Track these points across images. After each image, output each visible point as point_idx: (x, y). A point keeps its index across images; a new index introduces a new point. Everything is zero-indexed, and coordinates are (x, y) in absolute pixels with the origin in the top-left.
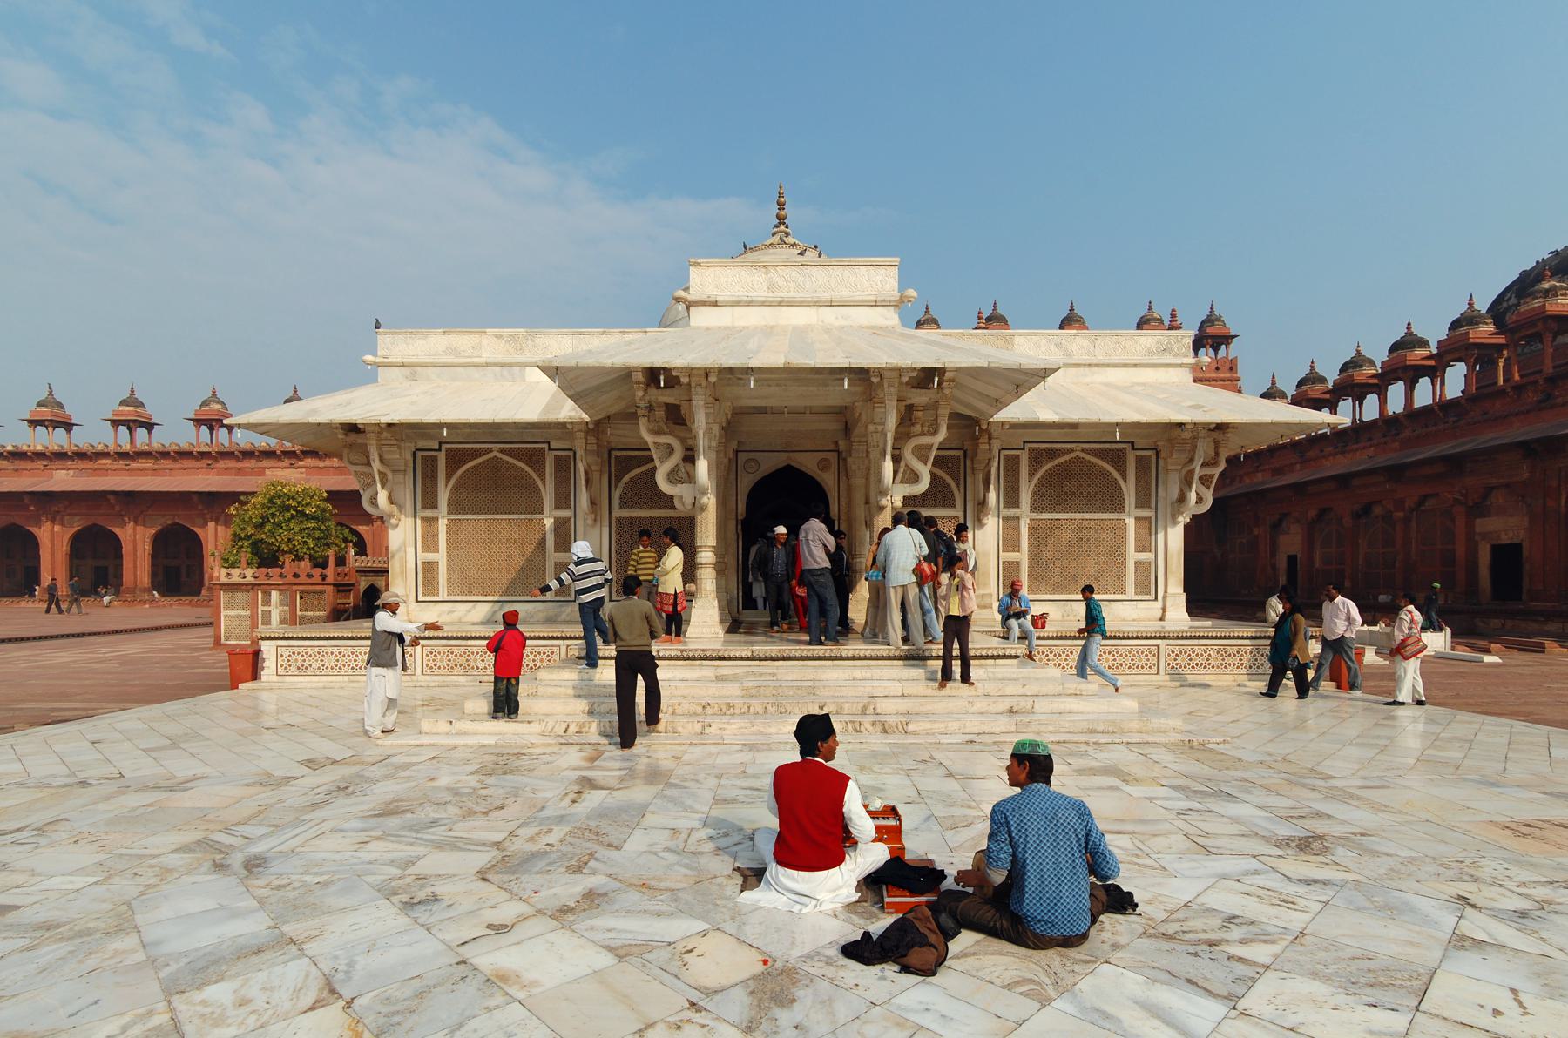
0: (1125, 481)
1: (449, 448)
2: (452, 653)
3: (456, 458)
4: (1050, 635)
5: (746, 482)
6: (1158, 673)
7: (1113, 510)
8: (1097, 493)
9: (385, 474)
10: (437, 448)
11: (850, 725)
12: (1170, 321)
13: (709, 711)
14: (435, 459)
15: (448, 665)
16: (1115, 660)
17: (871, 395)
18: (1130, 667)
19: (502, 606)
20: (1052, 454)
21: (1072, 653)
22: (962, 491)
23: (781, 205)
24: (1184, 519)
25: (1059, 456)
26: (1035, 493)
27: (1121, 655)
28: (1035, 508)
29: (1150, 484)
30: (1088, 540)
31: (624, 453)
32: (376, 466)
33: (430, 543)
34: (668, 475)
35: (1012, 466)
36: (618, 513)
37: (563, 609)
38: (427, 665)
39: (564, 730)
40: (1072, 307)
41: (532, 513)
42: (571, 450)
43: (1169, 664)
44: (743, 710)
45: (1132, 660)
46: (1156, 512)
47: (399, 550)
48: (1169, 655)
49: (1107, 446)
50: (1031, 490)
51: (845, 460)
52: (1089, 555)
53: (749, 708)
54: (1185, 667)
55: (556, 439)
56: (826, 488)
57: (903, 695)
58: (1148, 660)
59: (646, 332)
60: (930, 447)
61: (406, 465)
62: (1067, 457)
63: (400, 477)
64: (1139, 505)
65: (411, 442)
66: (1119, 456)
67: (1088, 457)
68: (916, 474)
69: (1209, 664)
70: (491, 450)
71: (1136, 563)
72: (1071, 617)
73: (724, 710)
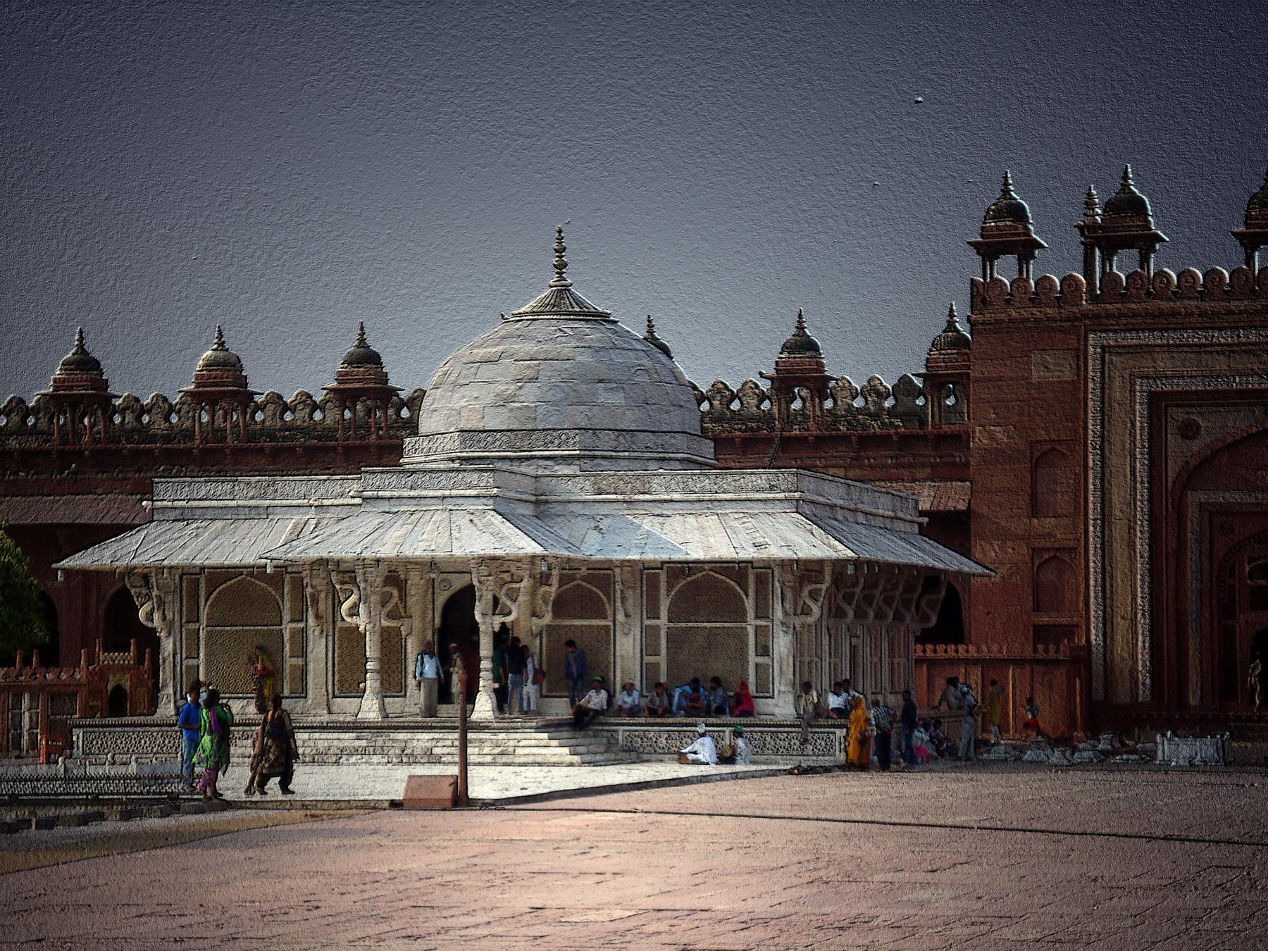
0: (747, 595)
5: (441, 599)
14: (198, 582)
22: (612, 604)
23: (560, 251)
50: (668, 604)
62: (699, 575)
64: (757, 617)
70: (241, 574)
71: (757, 665)
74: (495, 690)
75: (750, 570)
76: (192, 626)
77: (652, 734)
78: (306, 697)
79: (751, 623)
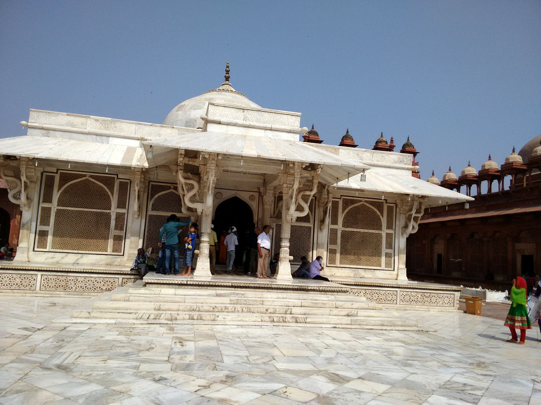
0: (383, 217)
1: (62, 173)
2: (58, 279)
3: (65, 178)
4: (352, 283)
6: (396, 304)
7: (377, 229)
8: (370, 221)
9: (27, 183)
10: (56, 172)
11: (281, 318)
12: (390, 143)
13: (216, 310)
14: (53, 178)
15: (55, 286)
16: (378, 297)
17: (286, 171)
18: (385, 300)
19: (82, 256)
20: (353, 202)
21: (360, 292)
24: (406, 236)
25: (356, 203)
26: (344, 219)
27: (381, 295)
28: (344, 226)
29: (393, 219)
30: (366, 241)
31: (156, 184)
32: (23, 179)
33: (45, 221)
34: (191, 197)
35: (335, 205)
36: (150, 212)
37: (116, 260)
38: (43, 285)
39: (147, 317)
40: (348, 131)
41: (105, 209)
42: (129, 180)
43: (401, 300)
44: (232, 310)
45: (386, 297)
46: (395, 231)
47: (26, 223)
48: (401, 296)
49: (376, 200)
51: (262, 197)
52: (366, 249)
53: (235, 309)
54: (408, 301)
55: (122, 173)
56: (252, 209)
57: (301, 306)
58: (392, 297)
59: (173, 127)
60: (309, 196)
61: (37, 179)
62: (359, 204)
63: (33, 185)
64: (387, 228)
65: (41, 168)
66: (380, 206)
67: (367, 205)
68: (303, 207)
69: (418, 301)
72: (358, 276)
73: (223, 310)
74: (290, 261)
75: (385, 204)
76: (46, 205)
77: (356, 291)
78: (123, 255)
79: (384, 232)
